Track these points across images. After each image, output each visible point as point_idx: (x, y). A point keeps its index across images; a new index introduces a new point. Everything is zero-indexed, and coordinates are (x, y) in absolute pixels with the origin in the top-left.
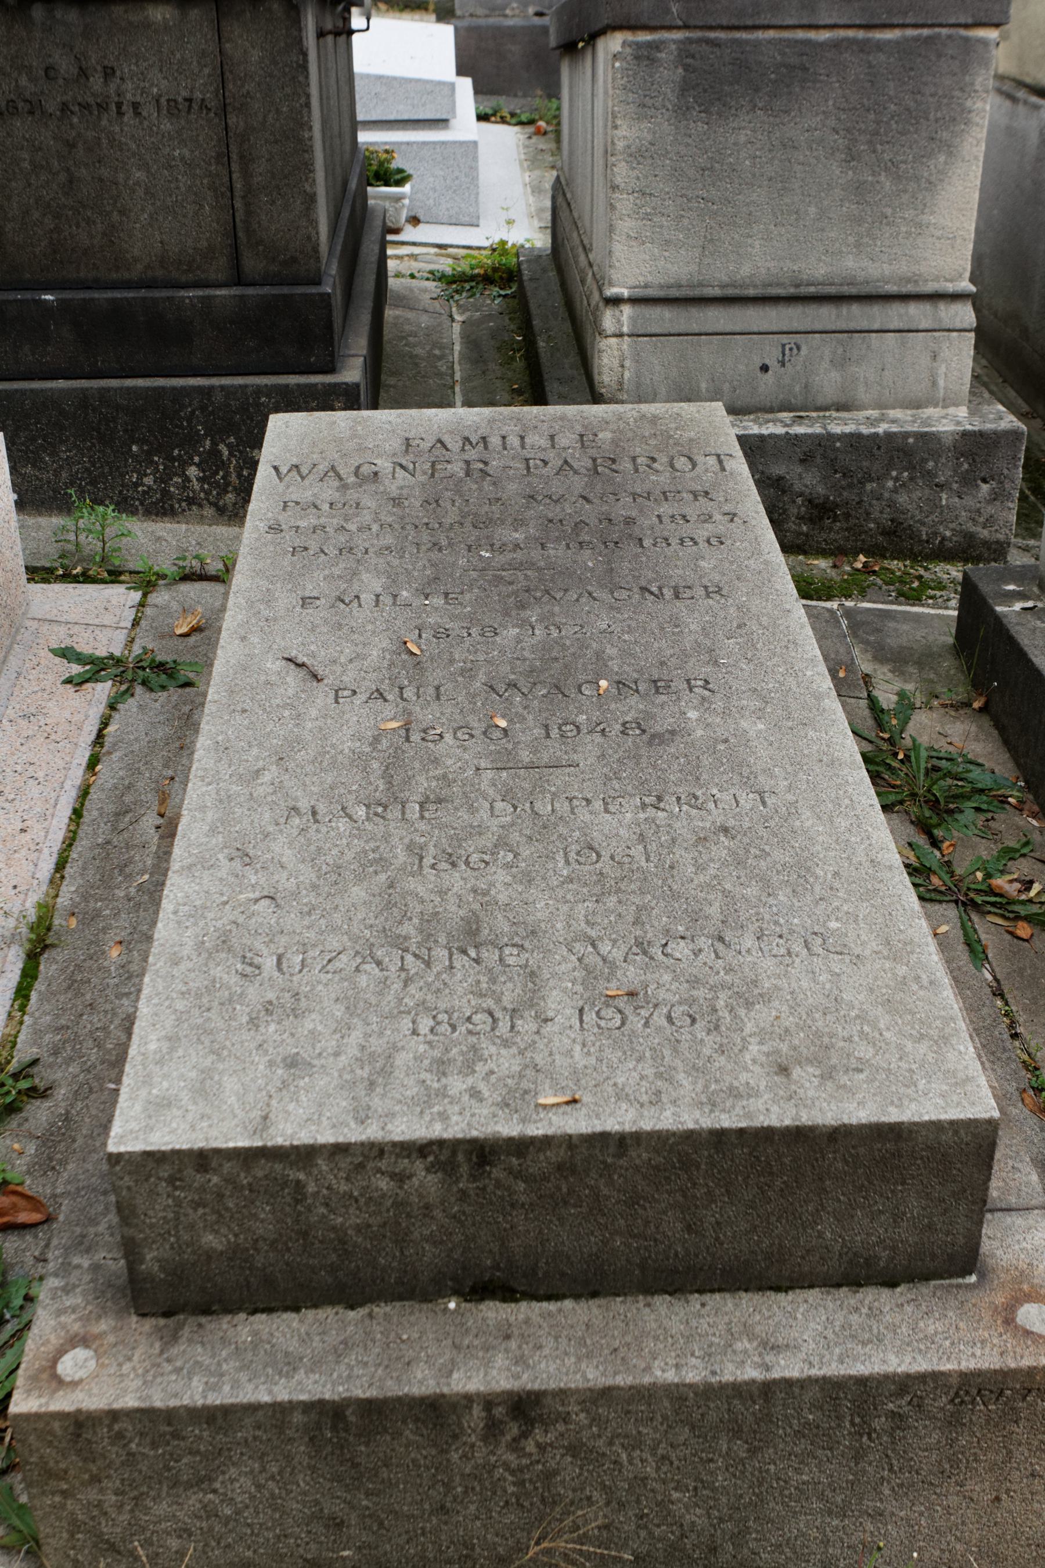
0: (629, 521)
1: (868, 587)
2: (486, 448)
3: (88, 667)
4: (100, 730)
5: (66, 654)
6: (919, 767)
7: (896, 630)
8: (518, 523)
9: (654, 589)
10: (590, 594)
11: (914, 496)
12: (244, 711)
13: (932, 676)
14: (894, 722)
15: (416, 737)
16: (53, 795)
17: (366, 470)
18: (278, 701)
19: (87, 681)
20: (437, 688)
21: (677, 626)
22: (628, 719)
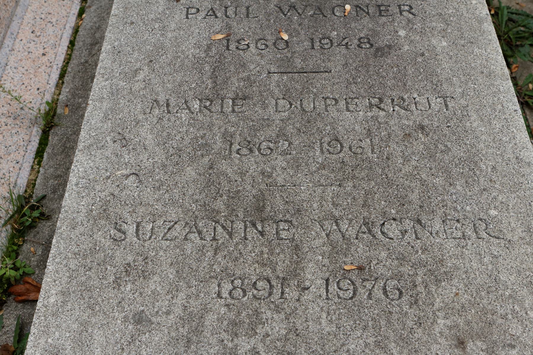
6: (502, 20)
12: (132, 23)
15: (233, 46)
16: (60, 32)
18: (152, 16)
20: (248, 8)
22: (362, 35)
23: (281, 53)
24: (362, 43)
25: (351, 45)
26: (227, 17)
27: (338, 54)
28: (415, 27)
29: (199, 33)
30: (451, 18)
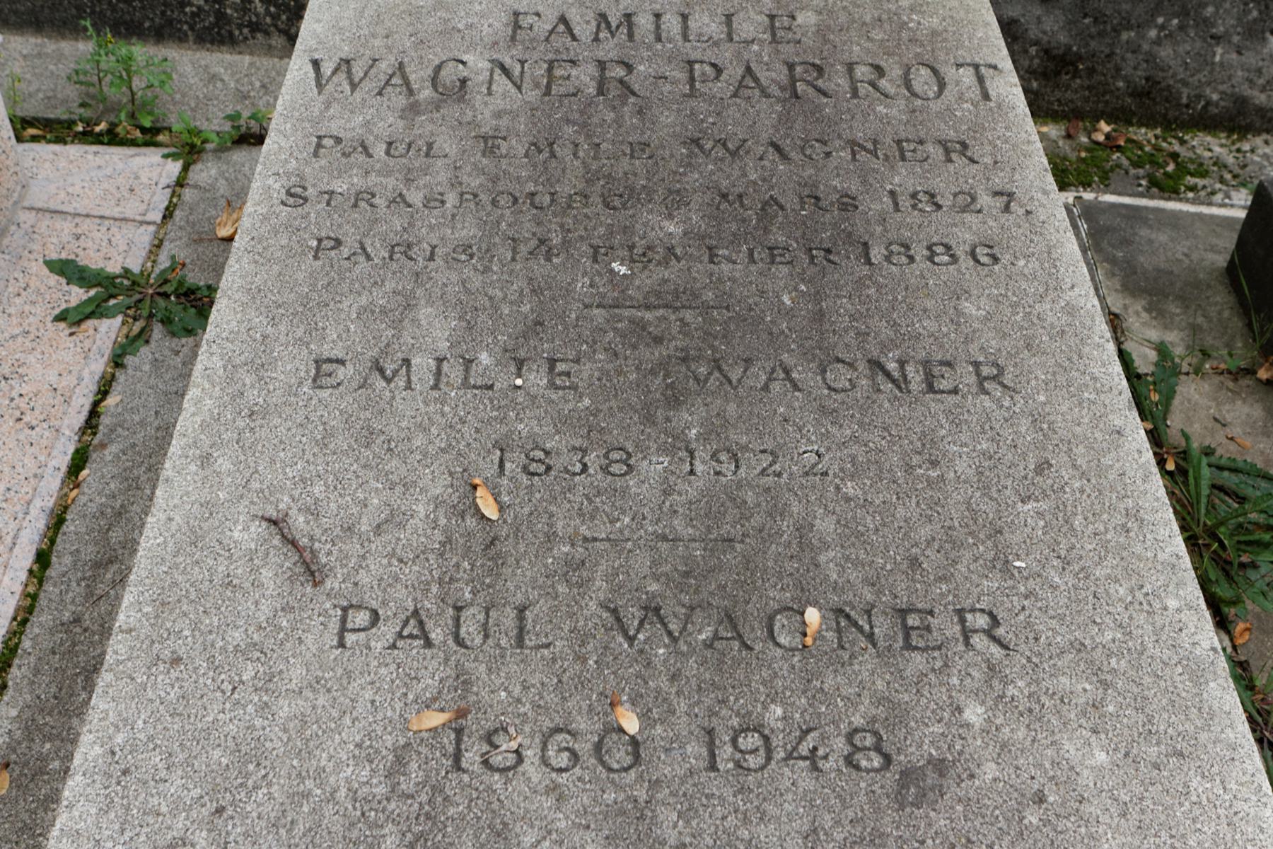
0: (848, 203)
1: (1112, 170)
2: (631, 36)
3: (92, 292)
4: (96, 404)
5: (67, 270)
6: (1198, 494)
7: (1150, 242)
8: (675, 201)
9: (892, 366)
10: (787, 372)
11: (1181, 49)
12: (176, 661)
13: (1200, 320)
14: (1155, 397)
15: (471, 758)
16: (13, 526)
17: (450, 74)
18: (236, 636)
19: (88, 317)
20: (521, 610)
21: (934, 464)
22: (858, 721)
23: (618, 787)
24: (858, 749)
25: (826, 757)
26: (460, 642)
27: (788, 790)
28: (1011, 691)
29: (373, 702)
30: (1113, 661)
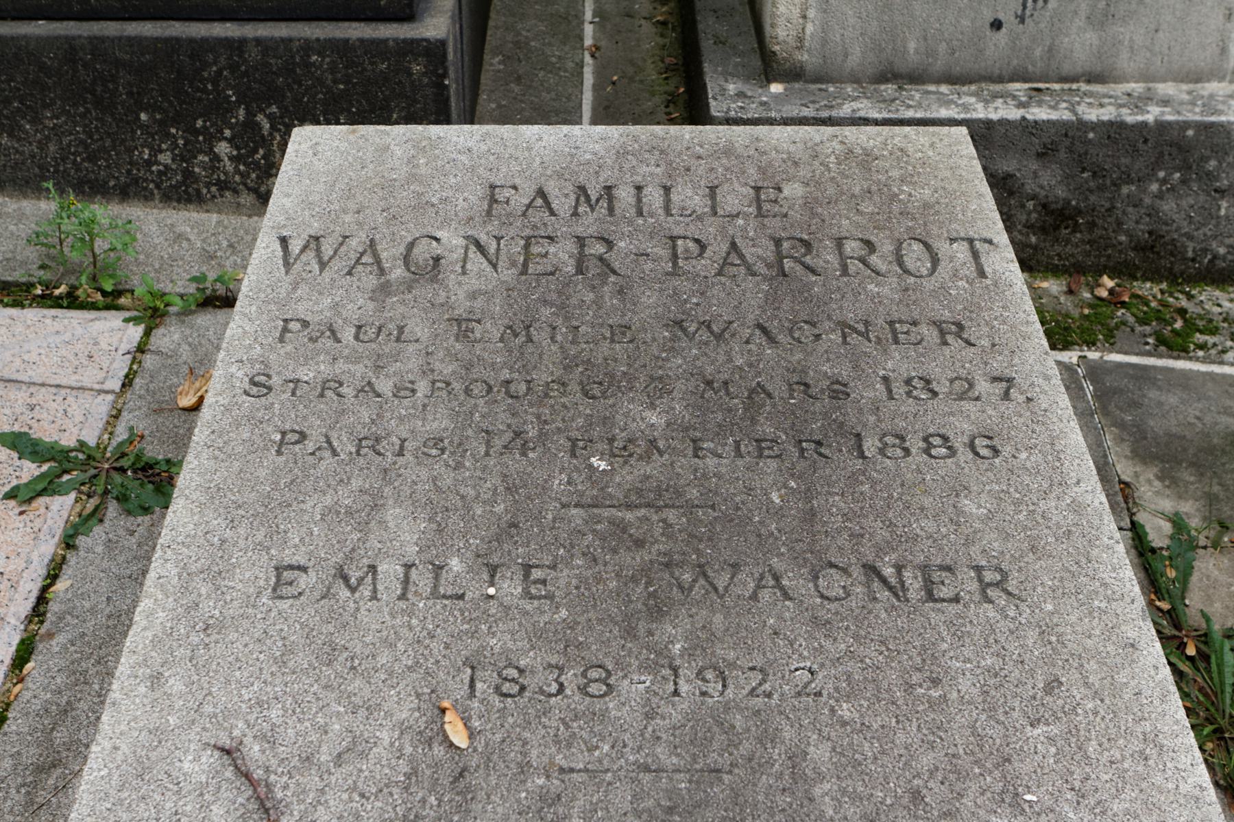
0: (839, 390)
1: (1117, 327)
2: (611, 210)
3: (45, 467)
4: (44, 589)
6: (1222, 683)
7: (1160, 404)
8: (658, 388)
9: (888, 571)
10: (777, 578)
11: (1184, 203)
13: (1216, 489)
14: (1172, 574)
17: (423, 251)
19: (40, 494)
21: (936, 682)
